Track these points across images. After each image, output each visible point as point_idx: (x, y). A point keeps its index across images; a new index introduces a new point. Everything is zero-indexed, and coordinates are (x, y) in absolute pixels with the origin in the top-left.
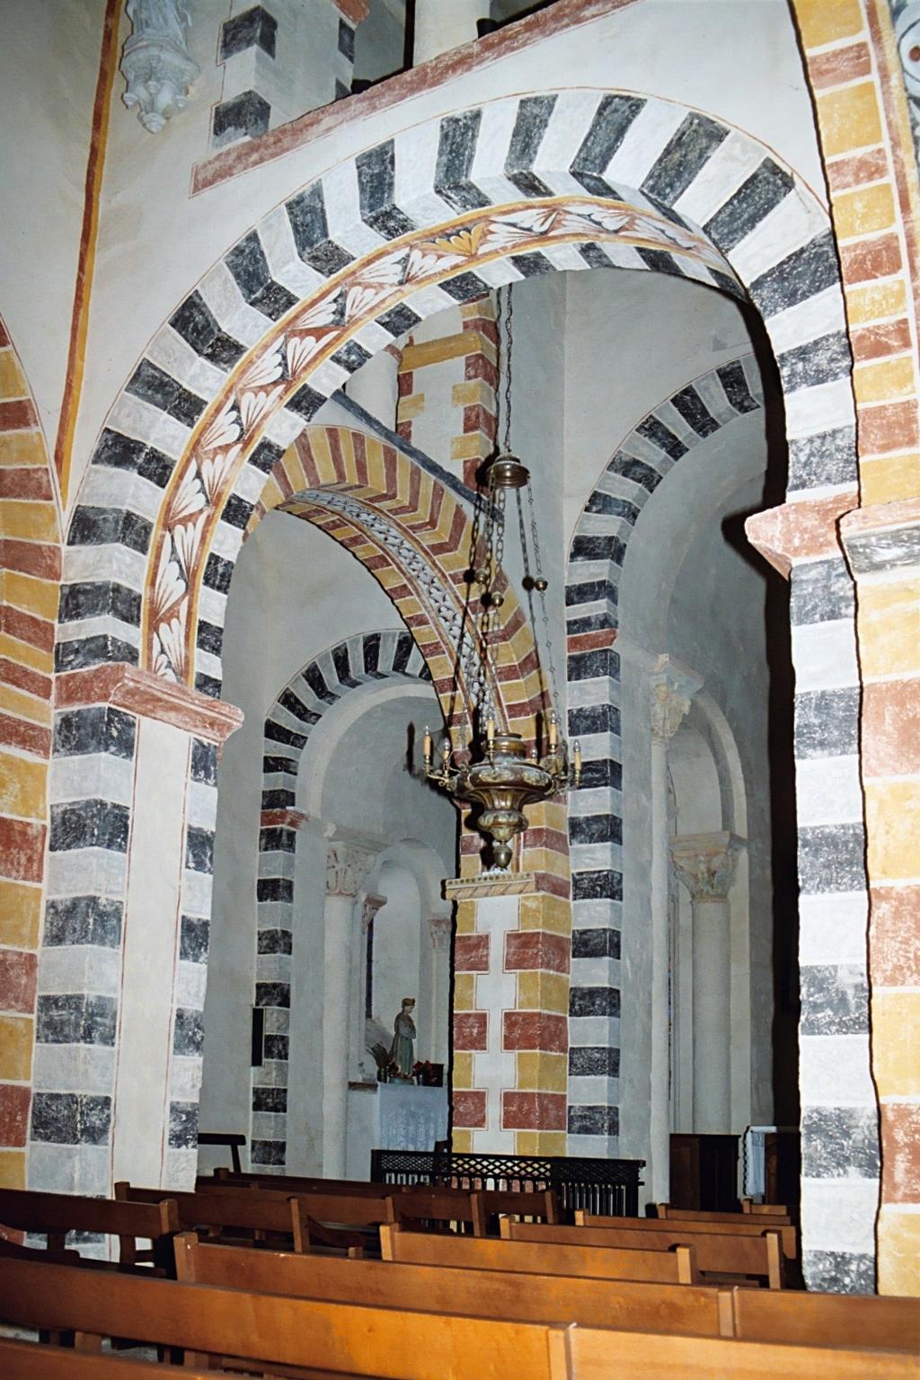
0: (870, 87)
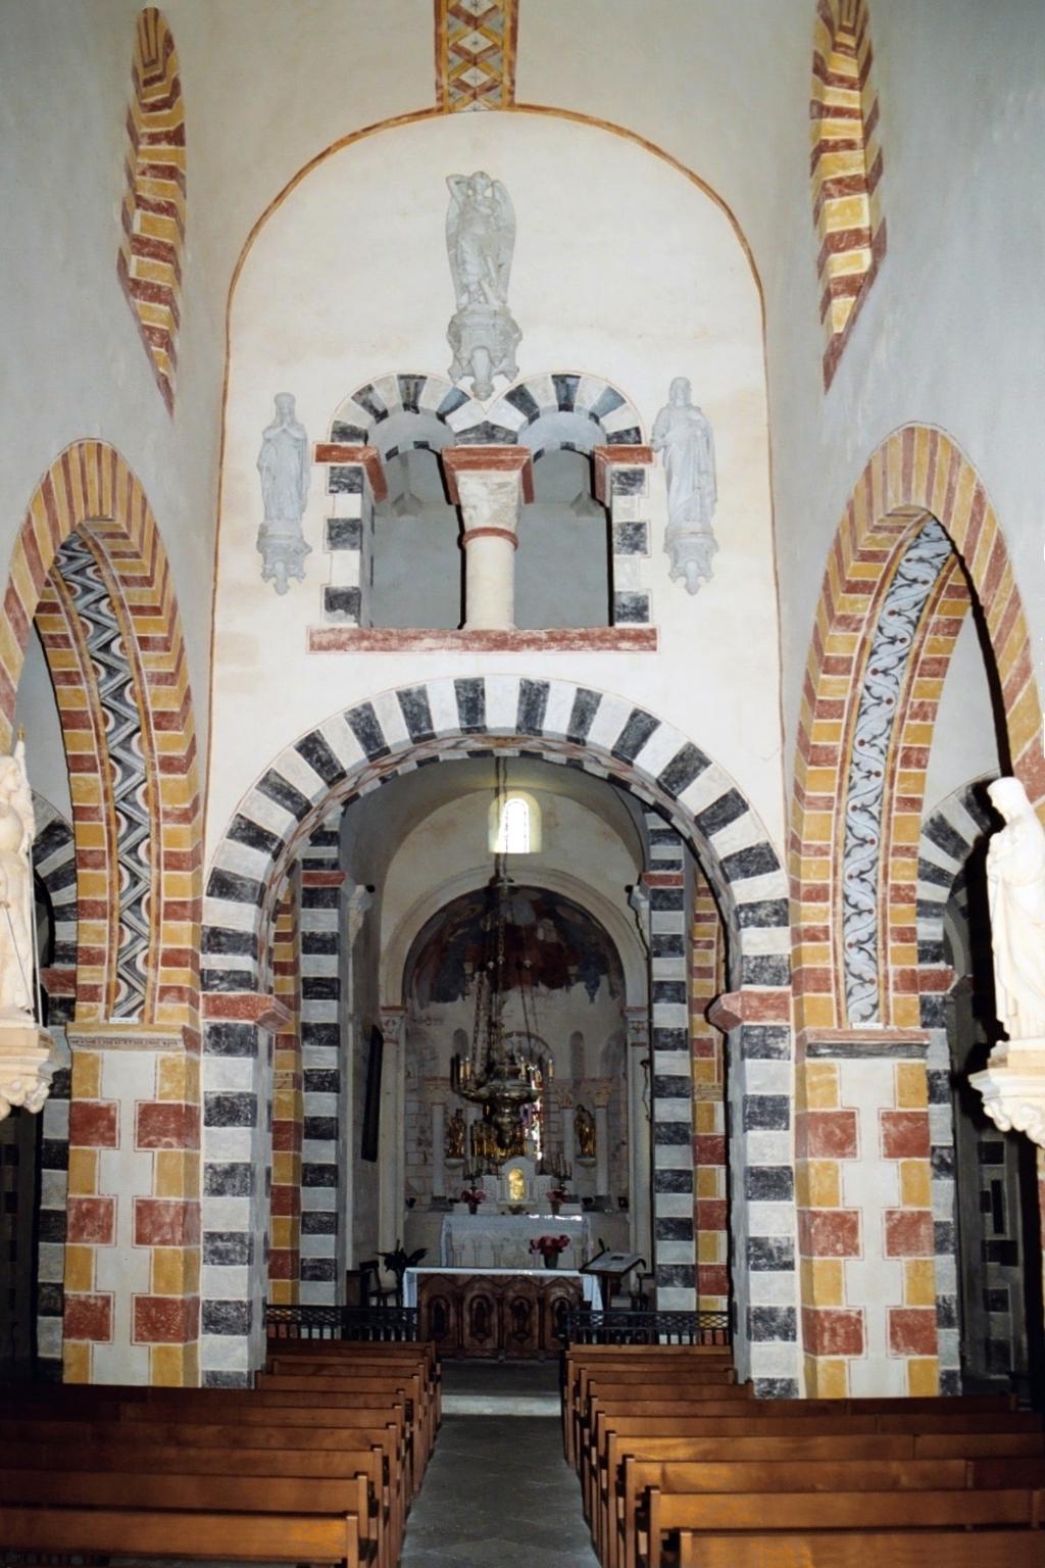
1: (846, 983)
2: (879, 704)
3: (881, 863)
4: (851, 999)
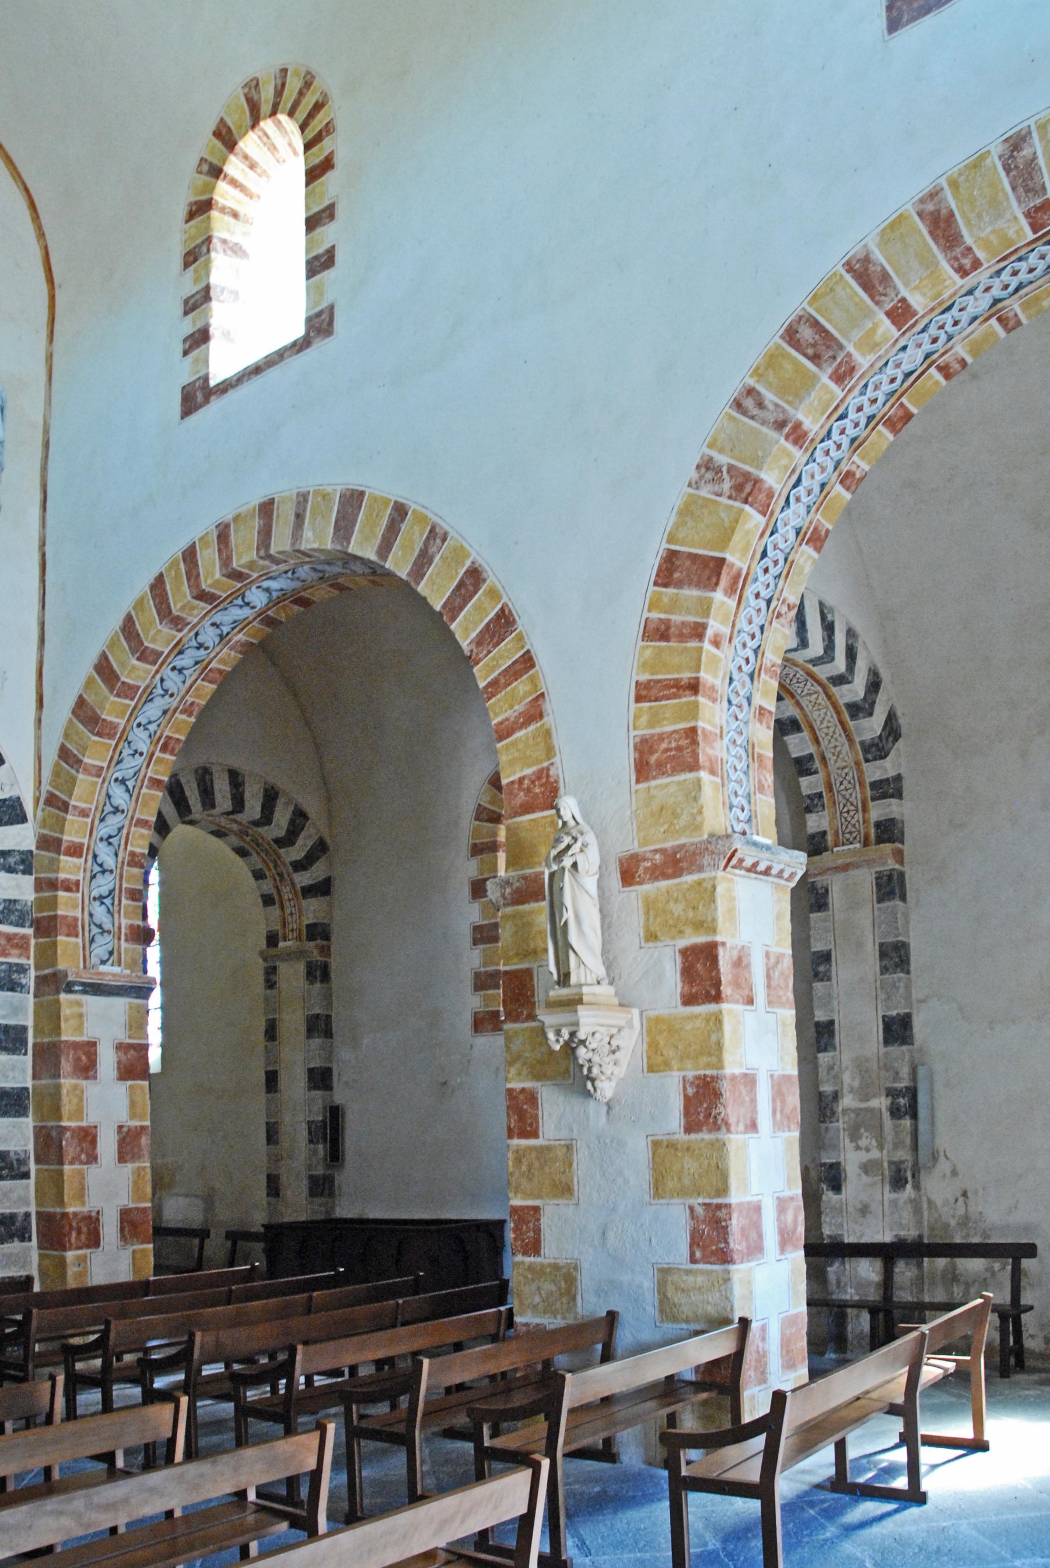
0: (97, 783)
2: (163, 696)
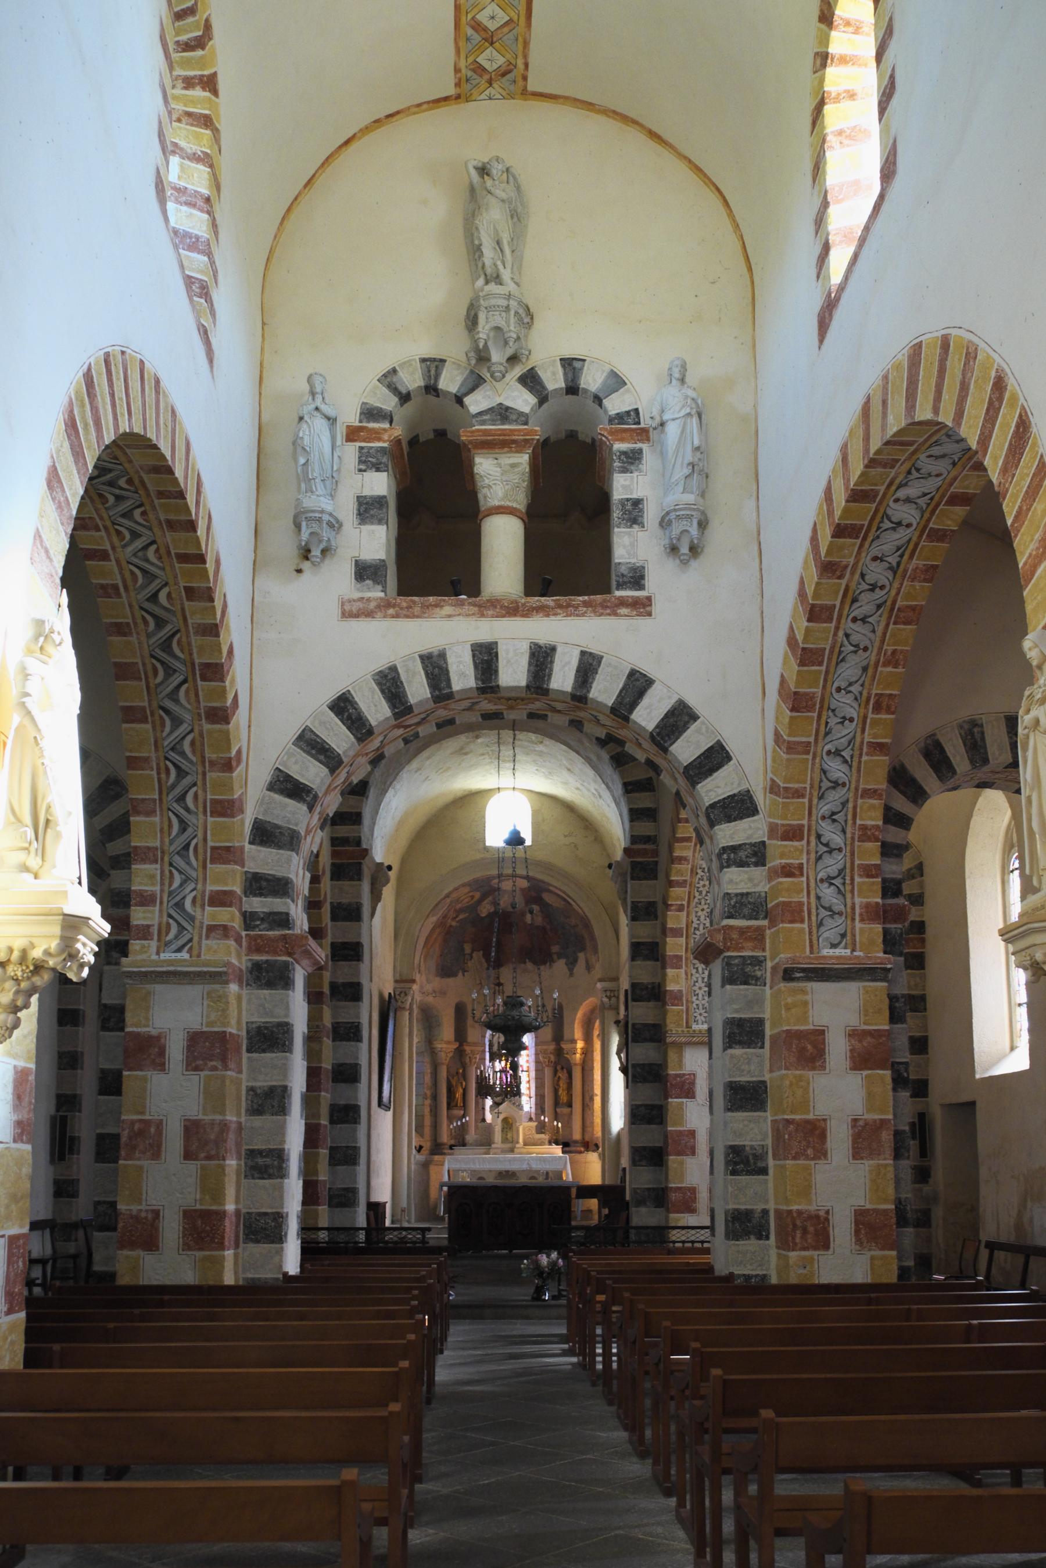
1: (817, 915)
2: (855, 652)
3: (850, 805)
4: (822, 929)
